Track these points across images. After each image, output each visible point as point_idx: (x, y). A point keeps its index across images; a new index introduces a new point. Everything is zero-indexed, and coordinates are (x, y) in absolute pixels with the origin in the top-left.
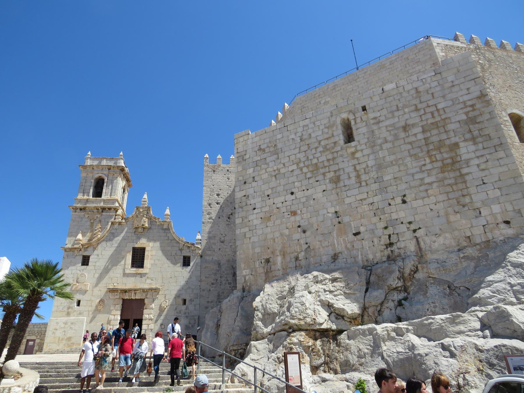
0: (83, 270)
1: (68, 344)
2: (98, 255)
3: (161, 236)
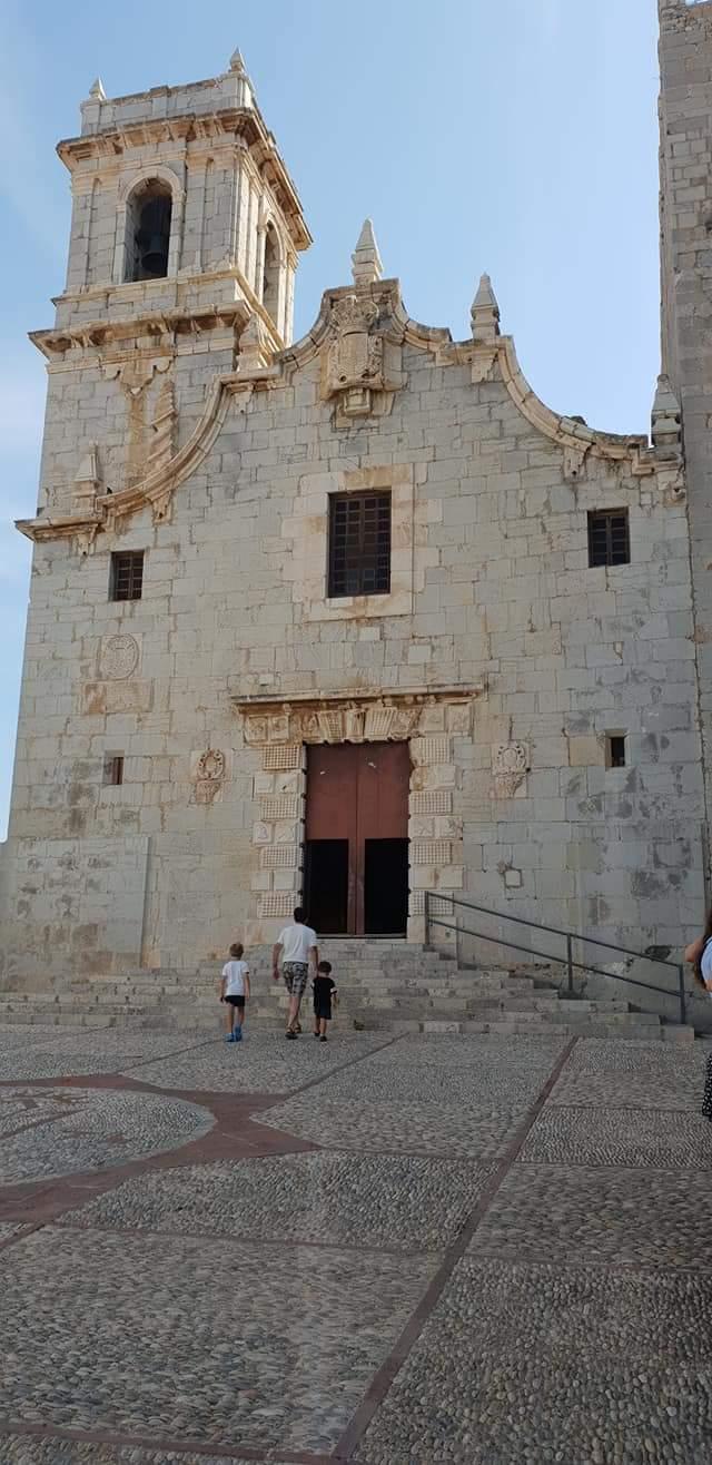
0: (120, 620)
1: (86, 957)
2: (177, 547)
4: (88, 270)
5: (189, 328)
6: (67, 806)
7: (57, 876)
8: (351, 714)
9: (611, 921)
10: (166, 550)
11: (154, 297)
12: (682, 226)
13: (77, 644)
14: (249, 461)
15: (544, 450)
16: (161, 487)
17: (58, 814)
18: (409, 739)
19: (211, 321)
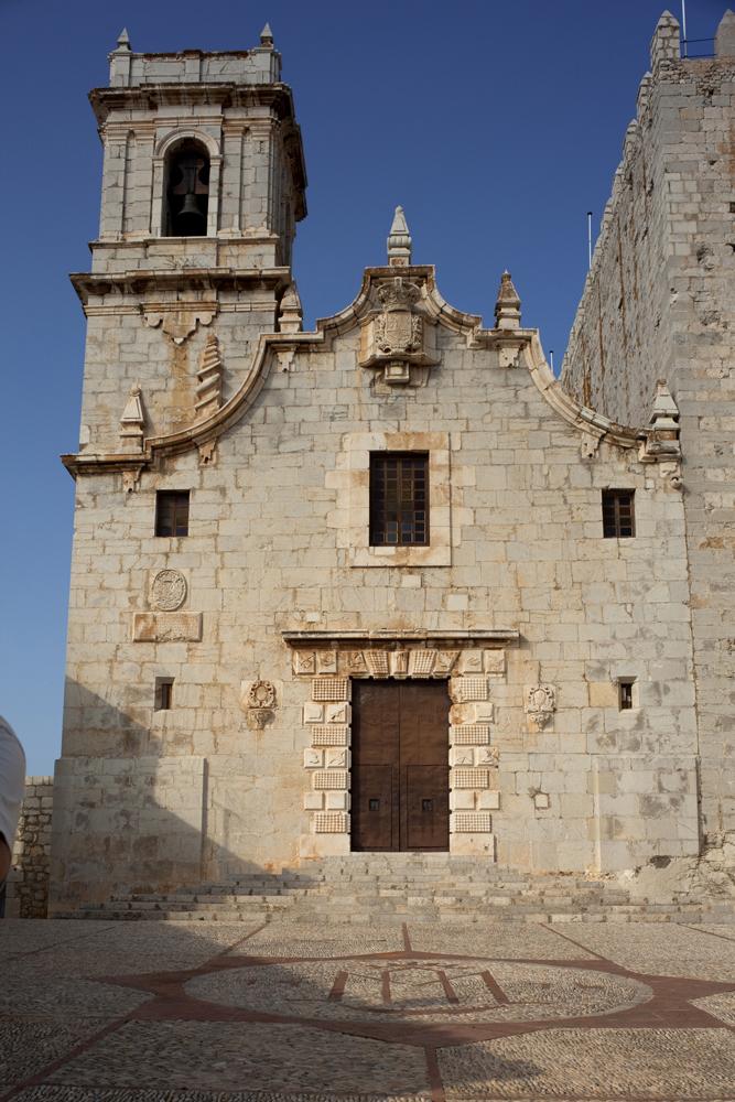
0: (167, 555)
2: (223, 491)
3: (491, 403)
4: (124, 219)
5: (232, 287)
6: (120, 728)
7: (114, 790)
8: (394, 655)
9: (623, 836)
11: (195, 255)
12: (678, 253)
13: (124, 577)
14: (293, 416)
15: (565, 432)
17: (112, 735)
18: (449, 678)
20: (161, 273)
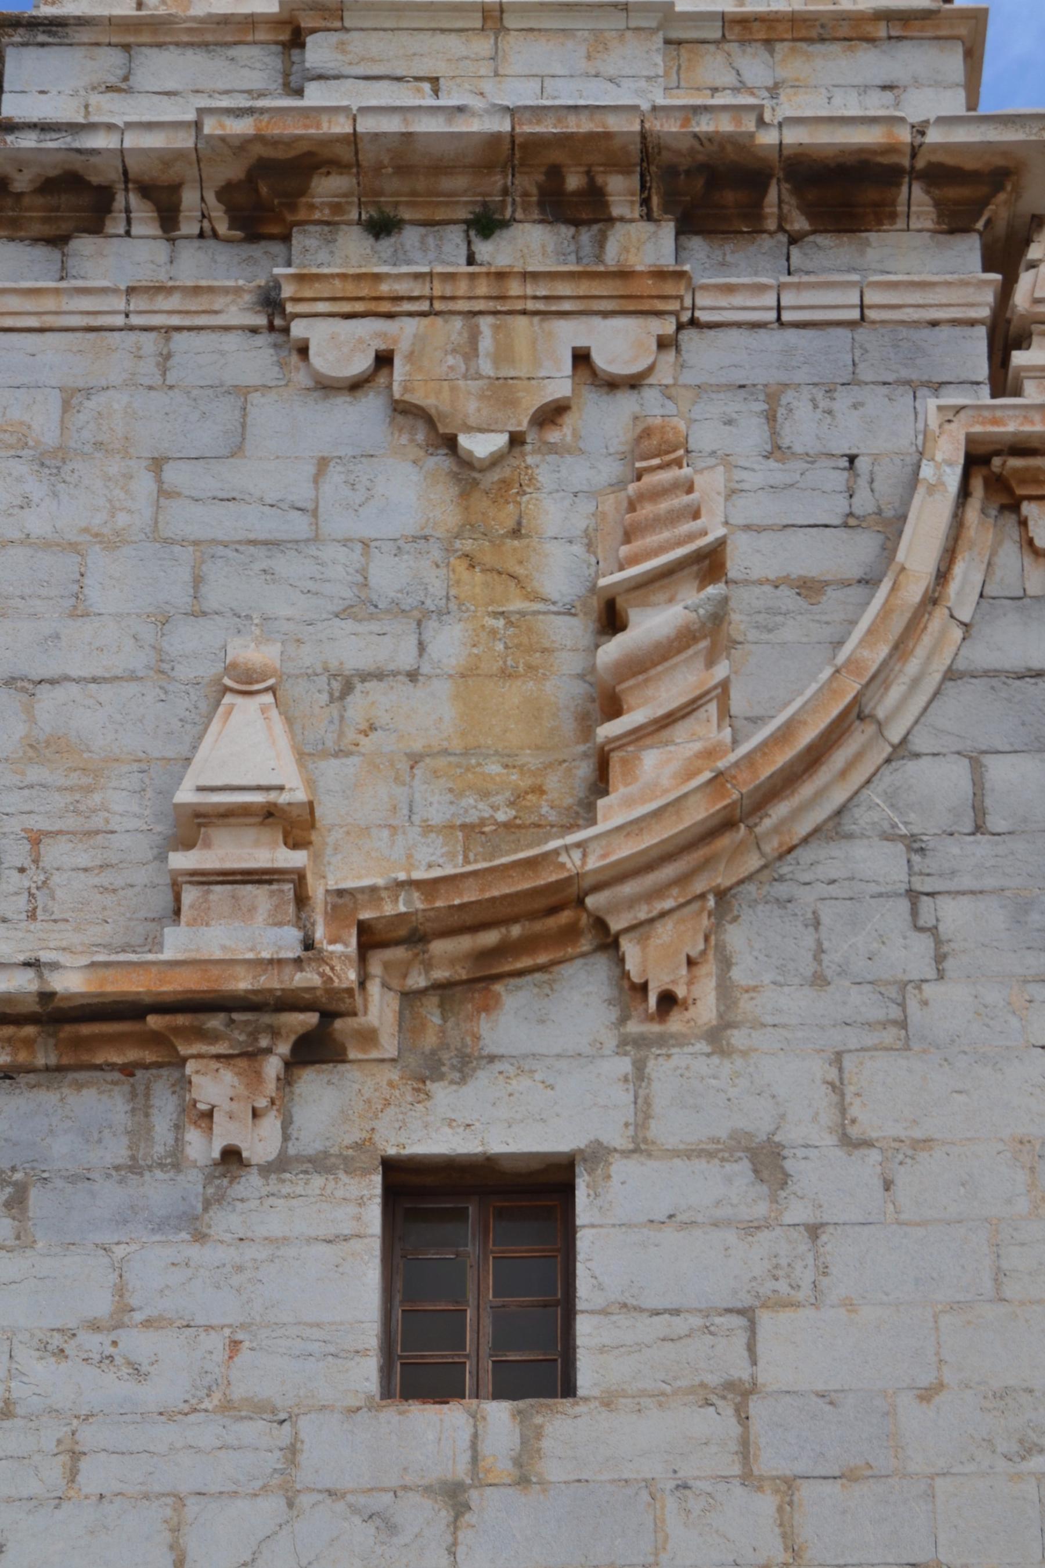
10: (701, 1164)
16: (668, 872)
19: (872, 194)
20: (392, 125)
